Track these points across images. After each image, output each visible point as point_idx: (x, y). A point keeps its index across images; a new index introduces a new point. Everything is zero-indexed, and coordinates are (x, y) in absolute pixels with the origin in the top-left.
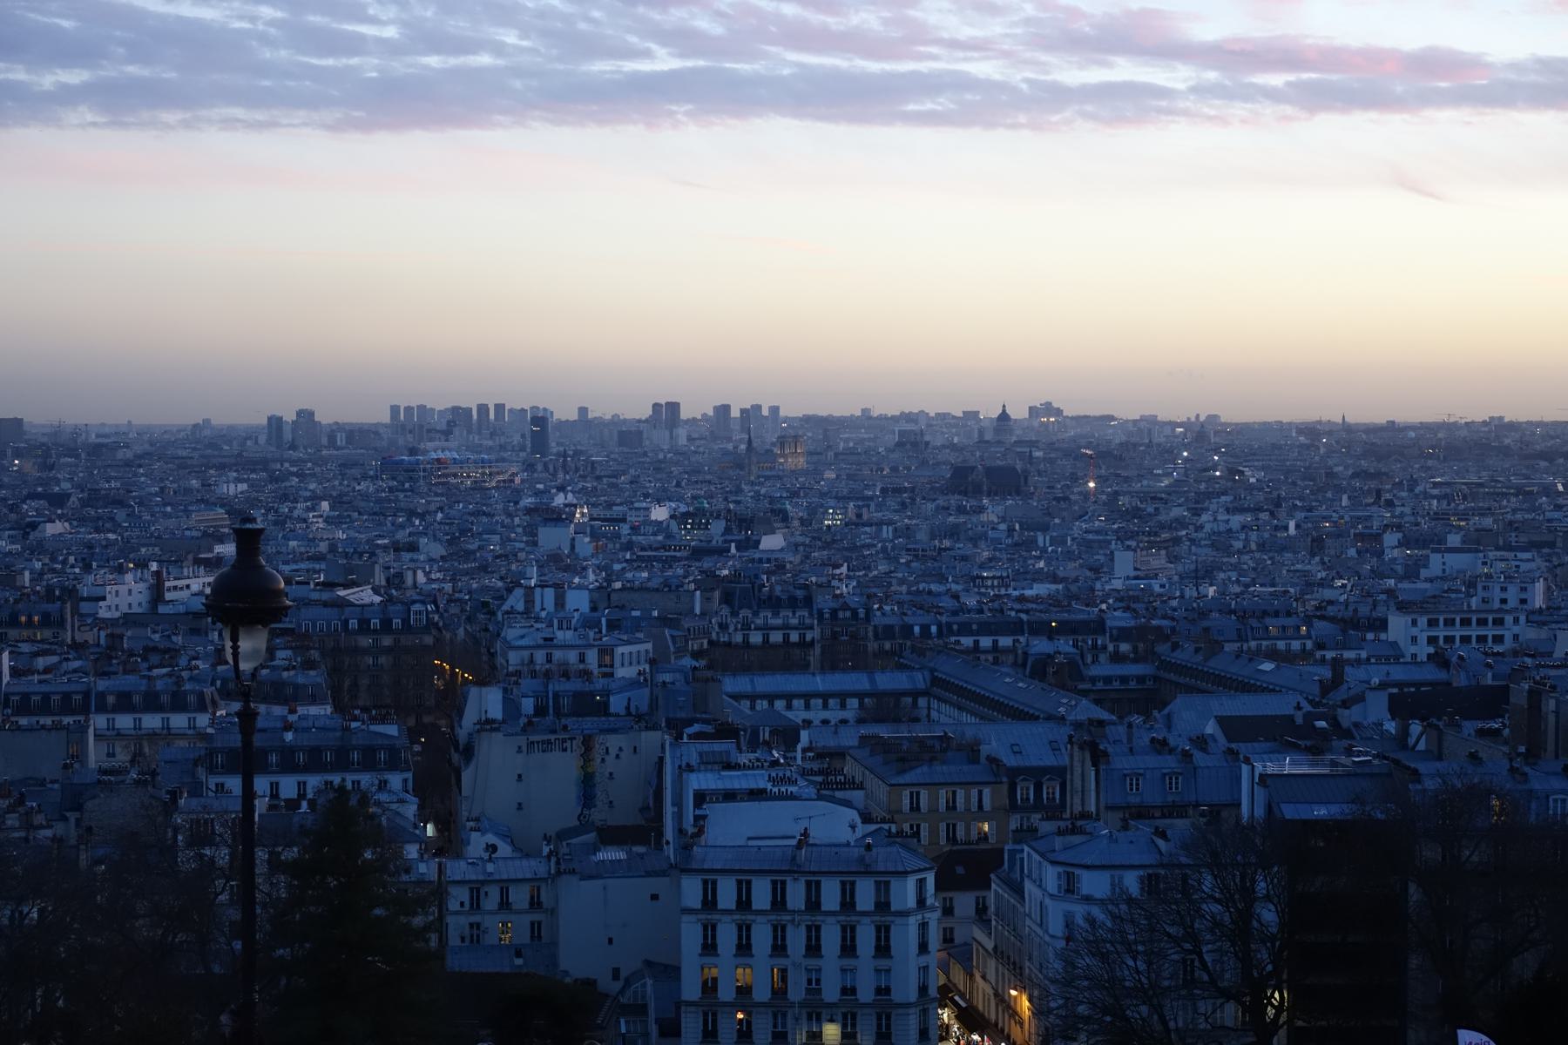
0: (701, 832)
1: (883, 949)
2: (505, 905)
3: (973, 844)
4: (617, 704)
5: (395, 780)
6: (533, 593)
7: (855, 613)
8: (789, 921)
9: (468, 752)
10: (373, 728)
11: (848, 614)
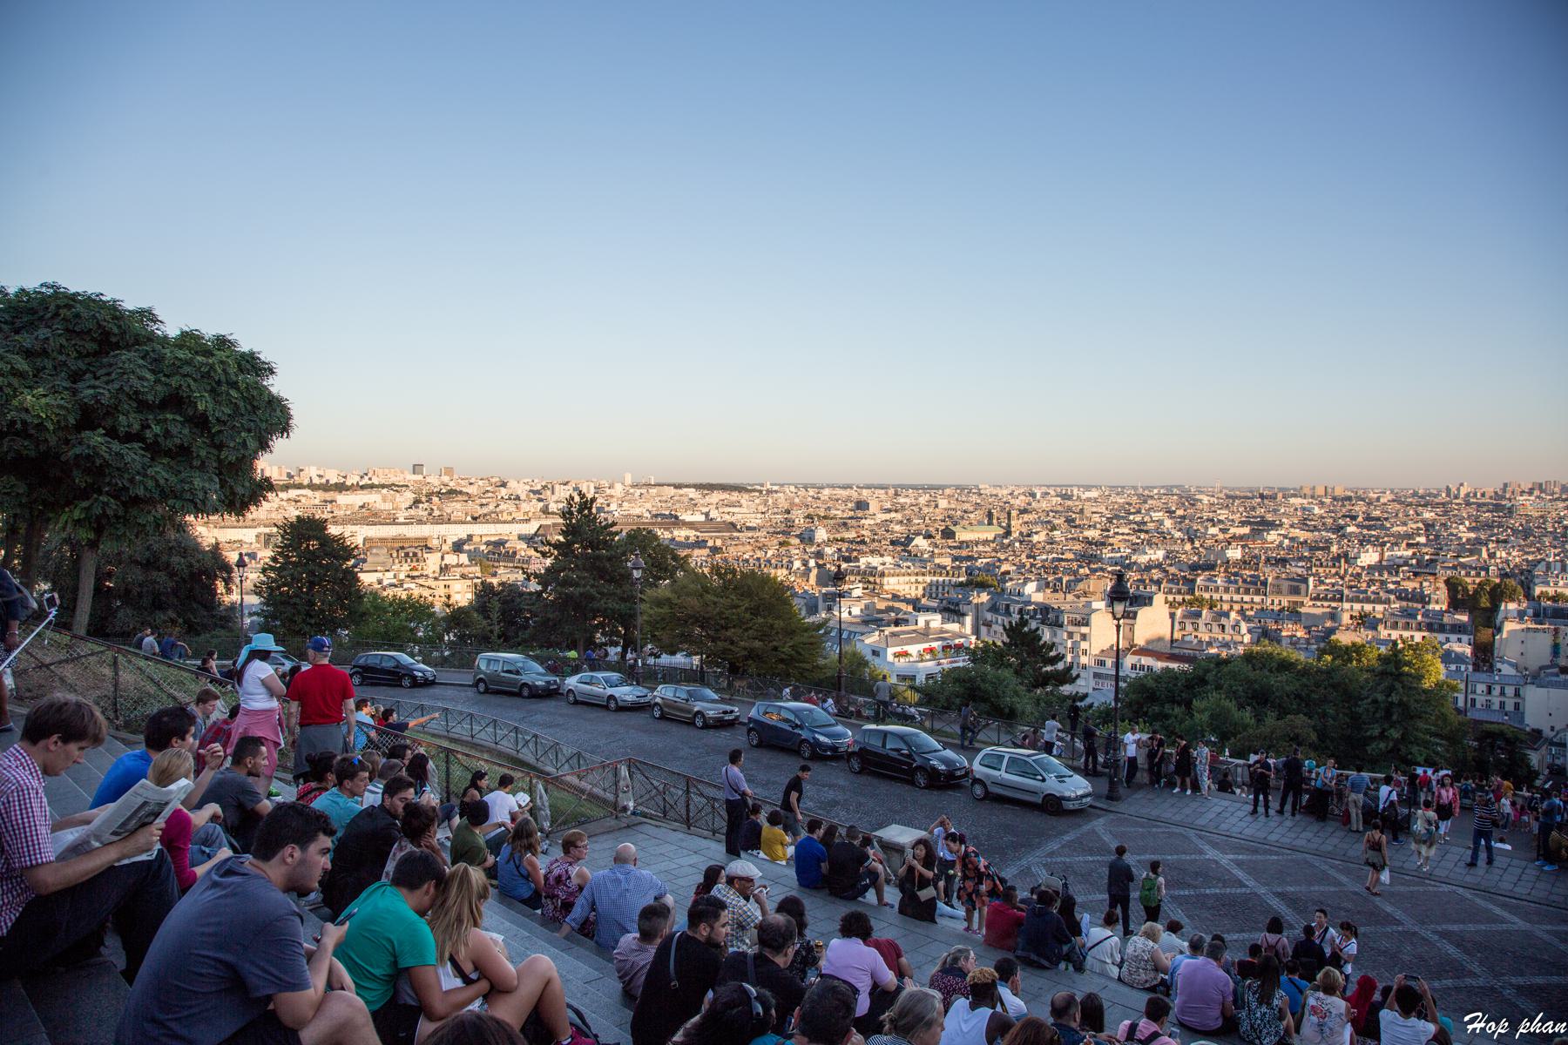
5: (1465, 638)
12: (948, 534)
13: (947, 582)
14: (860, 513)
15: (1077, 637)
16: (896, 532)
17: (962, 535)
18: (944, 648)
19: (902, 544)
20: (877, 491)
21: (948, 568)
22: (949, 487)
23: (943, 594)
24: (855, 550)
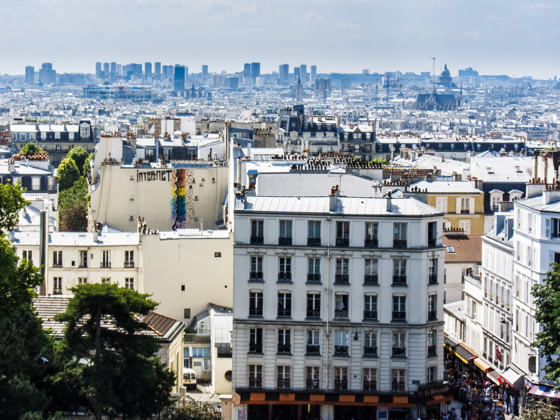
0: (252, 186)
2: (106, 264)
3: (460, 231)
4: (202, 154)
6: (160, 123)
7: (364, 135)
8: (322, 255)
9: (97, 180)
11: (360, 135)
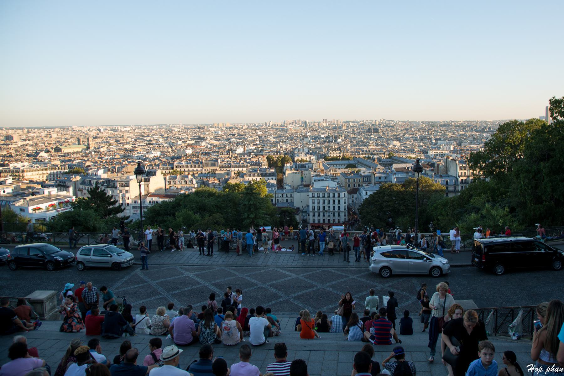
1: (339, 203)
2: (287, 196)
4: (307, 166)
5: (274, 178)
10: (271, 170)
12: (58, 150)
13: (59, 173)
14: (8, 142)
15: (124, 192)
16: (30, 150)
17: (65, 150)
18: (59, 203)
19: (33, 156)
20: (17, 131)
21: (59, 166)
22: (57, 127)
23: (57, 178)
24: (7, 160)
